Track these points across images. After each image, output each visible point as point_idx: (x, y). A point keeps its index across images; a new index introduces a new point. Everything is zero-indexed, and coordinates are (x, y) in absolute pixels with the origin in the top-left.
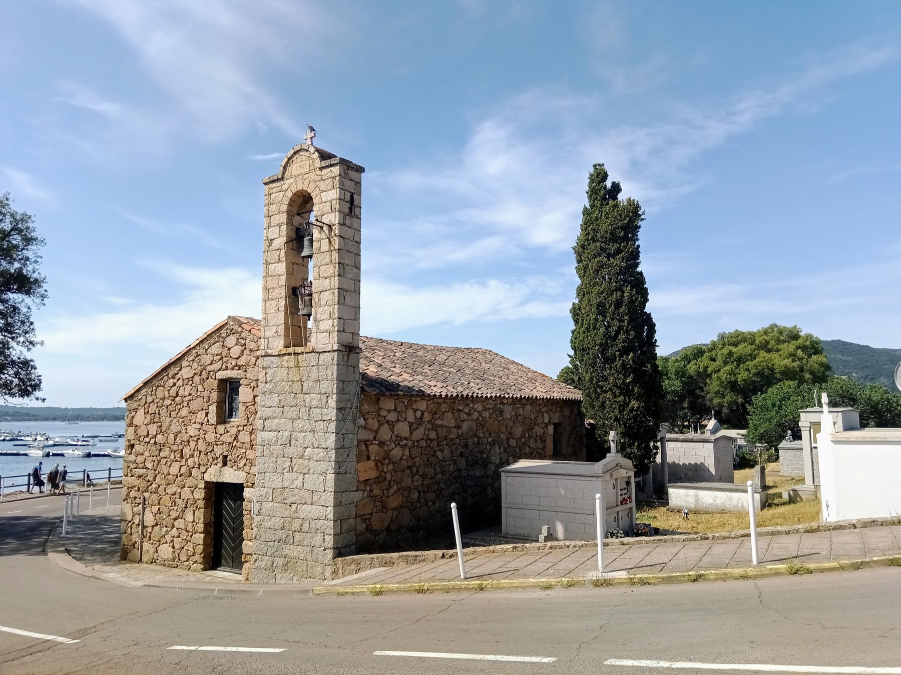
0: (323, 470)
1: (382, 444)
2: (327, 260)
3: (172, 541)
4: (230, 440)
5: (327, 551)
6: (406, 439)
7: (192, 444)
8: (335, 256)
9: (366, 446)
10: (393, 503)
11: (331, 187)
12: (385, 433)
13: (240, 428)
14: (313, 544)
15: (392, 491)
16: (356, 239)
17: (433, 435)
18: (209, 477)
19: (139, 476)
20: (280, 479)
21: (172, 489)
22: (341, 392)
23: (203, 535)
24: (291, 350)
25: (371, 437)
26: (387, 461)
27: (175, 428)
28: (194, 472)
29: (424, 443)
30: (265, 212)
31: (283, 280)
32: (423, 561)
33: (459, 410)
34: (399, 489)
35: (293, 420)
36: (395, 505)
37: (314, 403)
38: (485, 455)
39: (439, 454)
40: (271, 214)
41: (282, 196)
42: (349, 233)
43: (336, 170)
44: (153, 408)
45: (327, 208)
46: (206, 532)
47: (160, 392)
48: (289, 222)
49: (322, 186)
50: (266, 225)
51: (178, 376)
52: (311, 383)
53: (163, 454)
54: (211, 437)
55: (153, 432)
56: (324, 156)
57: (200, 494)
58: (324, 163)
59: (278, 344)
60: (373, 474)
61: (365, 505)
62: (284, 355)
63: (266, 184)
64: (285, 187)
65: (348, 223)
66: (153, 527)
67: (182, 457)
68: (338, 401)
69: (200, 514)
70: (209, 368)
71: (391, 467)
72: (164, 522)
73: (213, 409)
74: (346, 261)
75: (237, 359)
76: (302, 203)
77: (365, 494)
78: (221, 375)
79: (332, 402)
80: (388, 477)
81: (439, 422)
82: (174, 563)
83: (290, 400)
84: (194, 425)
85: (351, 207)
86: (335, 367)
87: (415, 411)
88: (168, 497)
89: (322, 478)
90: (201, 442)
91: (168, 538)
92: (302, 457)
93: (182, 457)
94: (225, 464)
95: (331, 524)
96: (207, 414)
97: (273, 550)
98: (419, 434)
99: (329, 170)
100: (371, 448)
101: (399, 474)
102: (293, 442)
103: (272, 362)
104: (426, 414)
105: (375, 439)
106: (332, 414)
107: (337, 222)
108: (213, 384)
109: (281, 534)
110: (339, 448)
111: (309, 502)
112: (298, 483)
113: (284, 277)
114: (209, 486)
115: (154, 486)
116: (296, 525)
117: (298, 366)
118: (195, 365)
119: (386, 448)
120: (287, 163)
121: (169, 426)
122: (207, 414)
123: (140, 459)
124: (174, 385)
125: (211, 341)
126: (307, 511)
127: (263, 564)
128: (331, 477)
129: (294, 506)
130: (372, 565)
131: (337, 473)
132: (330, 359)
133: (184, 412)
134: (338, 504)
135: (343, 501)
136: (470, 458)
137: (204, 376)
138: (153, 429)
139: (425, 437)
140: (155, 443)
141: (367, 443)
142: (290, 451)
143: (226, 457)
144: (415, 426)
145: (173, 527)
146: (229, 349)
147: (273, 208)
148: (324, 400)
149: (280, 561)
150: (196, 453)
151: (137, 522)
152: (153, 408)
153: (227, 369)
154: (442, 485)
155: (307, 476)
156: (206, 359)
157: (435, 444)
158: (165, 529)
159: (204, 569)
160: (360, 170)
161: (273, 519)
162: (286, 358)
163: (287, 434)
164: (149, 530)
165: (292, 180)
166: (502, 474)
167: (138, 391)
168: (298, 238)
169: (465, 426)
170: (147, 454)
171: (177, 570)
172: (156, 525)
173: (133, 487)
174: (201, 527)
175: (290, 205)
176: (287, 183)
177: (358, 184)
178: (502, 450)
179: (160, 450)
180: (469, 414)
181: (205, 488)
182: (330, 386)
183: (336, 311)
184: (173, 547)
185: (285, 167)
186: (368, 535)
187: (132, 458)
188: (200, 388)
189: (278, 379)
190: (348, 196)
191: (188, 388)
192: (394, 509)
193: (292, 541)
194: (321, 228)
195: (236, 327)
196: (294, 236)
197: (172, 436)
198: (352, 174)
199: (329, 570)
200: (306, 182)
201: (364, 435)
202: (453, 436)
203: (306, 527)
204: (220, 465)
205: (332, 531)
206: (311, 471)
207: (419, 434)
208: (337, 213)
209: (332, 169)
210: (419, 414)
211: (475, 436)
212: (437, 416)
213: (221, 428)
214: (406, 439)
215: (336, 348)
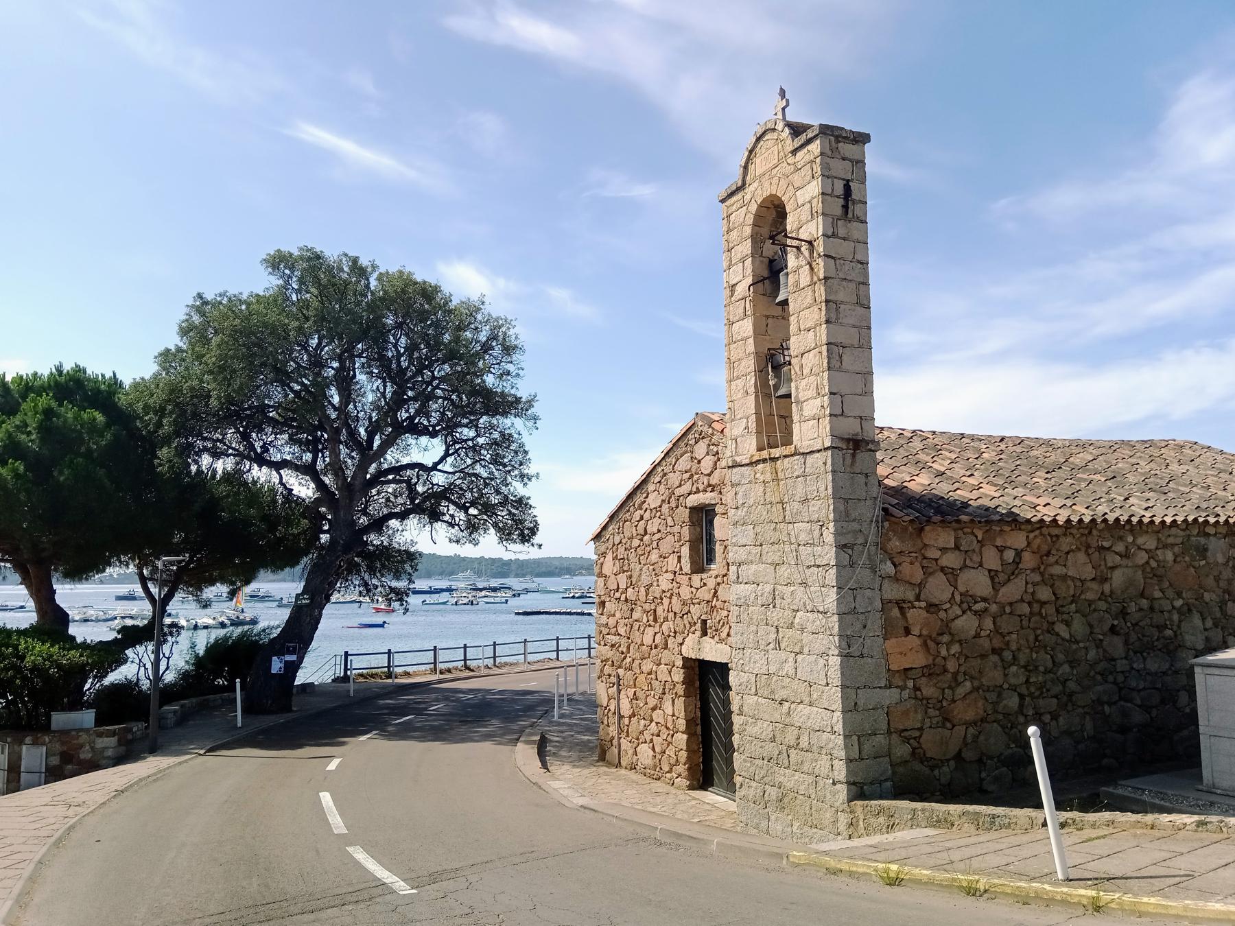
0: (823, 649)
1: (932, 607)
2: (809, 300)
3: (652, 740)
4: (708, 597)
5: (839, 786)
6: (984, 600)
7: (666, 601)
8: (821, 289)
9: (901, 609)
10: (966, 711)
11: (808, 178)
12: (938, 588)
13: (719, 580)
14: (817, 772)
15: (961, 691)
16: (859, 257)
17: (1044, 594)
18: (689, 651)
19: (613, 646)
20: (764, 661)
21: (648, 666)
22: (843, 516)
23: (685, 736)
24: (765, 454)
25: (910, 595)
26: (945, 638)
27: (646, 579)
28: (670, 641)
29: (1025, 609)
30: (724, 246)
31: (751, 347)
32: (1008, 826)
33: (1101, 549)
34: (975, 689)
35: (776, 565)
36: (970, 715)
37: (803, 537)
38: (1169, 633)
39: (1061, 629)
40: (731, 245)
41: (744, 214)
42: (844, 249)
43: (815, 147)
44: (621, 553)
45: (805, 213)
46: (689, 731)
47: (629, 529)
48: (757, 252)
49: (797, 179)
50: (725, 265)
51: (645, 506)
52: (796, 506)
53: (636, 616)
54: (685, 592)
55: (623, 586)
56: (797, 130)
57: (678, 676)
58: (798, 142)
59: (749, 447)
60: (918, 660)
61: (906, 713)
62: (758, 462)
63: (723, 201)
64: (748, 197)
65: (842, 232)
66: (630, 717)
67: (655, 620)
68: (837, 534)
69: (680, 703)
70: (678, 492)
71: (955, 648)
72: (641, 712)
73: (685, 551)
74: (841, 296)
75: (709, 475)
76: (773, 216)
77: (906, 694)
78: (693, 500)
79: (829, 537)
80: (951, 666)
81: (1058, 570)
82: (655, 773)
83: (768, 533)
84: (666, 575)
85: (846, 203)
86: (830, 476)
87: (1001, 550)
88: (643, 676)
89: (822, 662)
90: (675, 598)
91: (647, 736)
92: (791, 626)
93: (655, 620)
94: (704, 633)
95: (840, 740)
96: (679, 557)
97: (763, 772)
98: (1012, 591)
99: (805, 150)
100: (911, 614)
101: (976, 663)
102: (778, 602)
103: (742, 475)
104: (1026, 556)
105: (918, 599)
106: (829, 554)
107: (820, 233)
108: (683, 514)
109: (771, 749)
110: (846, 614)
111: (806, 701)
112: (789, 668)
113: (751, 341)
114: (689, 664)
115: (628, 660)
116: (790, 739)
117: (776, 479)
118: (662, 489)
119: (942, 614)
120: (748, 159)
121: (640, 576)
122: (679, 557)
123: (612, 622)
124: (642, 518)
125: (678, 452)
126: (803, 714)
127: (751, 792)
128: (835, 661)
129: (786, 705)
130: (913, 823)
131: (846, 656)
132: (821, 463)
133: (654, 557)
134: (850, 709)
135: (861, 703)
136: (1133, 637)
137: (673, 504)
138: (623, 580)
139: (1028, 598)
140: (626, 600)
141: (900, 604)
142: (775, 616)
143: (704, 622)
144: (1002, 577)
145: (652, 721)
146: (699, 462)
147: (734, 234)
148: (816, 533)
149: (773, 793)
150: (671, 615)
151: (613, 709)
152: (621, 553)
153: (698, 491)
154: (1072, 685)
155: (800, 657)
156: (674, 479)
157: (1051, 610)
158: (643, 722)
159: (691, 788)
160: (861, 139)
161: (759, 723)
162: (760, 466)
163: (768, 588)
164: (626, 721)
165: (755, 185)
166: (1197, 670)
167: (605, 528)
168: (770, 275)
169: (1118, 577)
170: (618, 615)
171: (658, 783)
172: (633, 715)
173: (607, 660)
174: (682, 724)
175: (755, 225)
176: (749, 190)
177: (860, 163)
178: (1209, 623)
179: (632, 610)
180: (1125, 556)
181: (684, 667)
182: (823, 508)
183: (826, 382)
184: (653, 749)
185: (746, 167)
186: (917, 766)
187: (604, 619)
188: (670, 522)
189: (751, 502)
190: (839, 188)
191: (657, 521)
192: (968, 724)
193: (786, 761)
194: (798, 248)
195: (706, 428)
196: (766, 274)
197: (643, 590)
198: (847, 149)
199: (843, 819)
200: (775, 180)
201: (893, 591)
202: (1090, 596)
203: (804, 743)
204: (698, 633)
205: (843, 754)
206: (806, 650)
207: (1012, 591)
208: (820, 218)
209: (810, 147)
210: (1010, 556)
211: (1142, 595)
212: (1052, 559)
213: (696, 579)
214: (984, 600)
215: (828, 444)
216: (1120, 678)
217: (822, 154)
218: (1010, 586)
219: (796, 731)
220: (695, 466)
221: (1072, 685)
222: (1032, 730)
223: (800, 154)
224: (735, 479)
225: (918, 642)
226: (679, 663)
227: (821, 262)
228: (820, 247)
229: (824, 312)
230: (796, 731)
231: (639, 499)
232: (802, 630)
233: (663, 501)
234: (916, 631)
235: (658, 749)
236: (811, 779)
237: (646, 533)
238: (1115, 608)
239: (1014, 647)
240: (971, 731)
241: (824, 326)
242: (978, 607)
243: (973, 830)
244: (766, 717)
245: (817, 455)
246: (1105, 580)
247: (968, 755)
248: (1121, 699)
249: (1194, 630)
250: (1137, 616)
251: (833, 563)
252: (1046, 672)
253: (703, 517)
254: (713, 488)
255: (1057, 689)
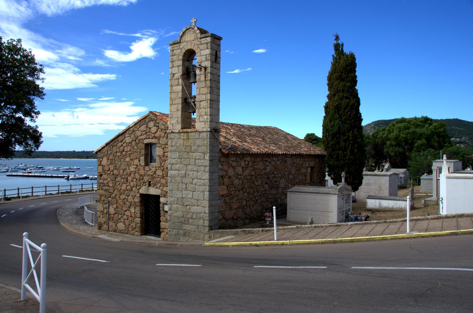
0: (203, 190)
1: (230, 177)
2: (204, 85)
3: (124, 221)
4: (151, 174)
5: (206, 228)
6: (241, 175)
7: (132, 175)
8: (208, 83)
9: (222, 178)
10: (235, 206)
11: (206, 48)
12: (231, 172)
13: (157, 168)
14: (198, 224)
15: (234, 200)
16: (218, 74)
17: (253, 173)
18: (141, 191)
19: (106, 190)
20: (181, 194)
21: (123, 197)
22: (211, 151)
23: (140, 219)
24: (185, 130)
25: (225, 174)
26: (232, 186)
27: (123, 167)
28: (134, 189)
29: (249, 177)
30: (170, 60)
31: (180, 95)
32: (253, 233)
33: (266, 161)
34: (237, 199)
35: (187, 165)
36: (236, 207)
37: (198, 157)
38: (277, 183)
39: (256, 182)
40: (173, 60)
41: (180, 52)
42: (216, 71)
43: (209, 39)
44: (111, 157)
45: (204, 58)
46: (141, 217)
47: (115, 149)
48: (183, 65)
49: (201, 47)
50: (171, 66)
51: (124, 141)
52: (196, 147)
53: (117, 180)
54: (142, 172)
55: (112, 169)
56: (203, 32)
57: (137, 200)
58: (202, 36)
59: (178, 127)
60: (225, 192)
61: (222, 207)
62: (181, 132)
63: (171, 45)
64: (181, 47)
65: (214, 67)
66: (114, 214)
67: (127, 181)
68: (210, 157)
69: (138, 209)
70: (140, 138)
71: (234, 189)
72: (120, 212)
73: (142, 158)
74: (214, 86)
75: (154, 133)
76: (190, 55)
77: (222, 201)
78: (146, 141)
79: (207, 157)
80: (232, 193)
81: (256, 167)
82: (125, 231)
83: (185, 155)
84: (133, 166)
85: (216, 58)
86: (209, 140)
87: (245, 161)
88: (121, 200)
89: (202, 194)
90: (137, 174)
91: (122, 220)
92: (192, 183)
93: (127, 181)
94: (150, 185)
95: (207, 215)
96: (139, 161)
97: (178, 227)
98: (247, 172)
99: (205, 39)
100: (225, 179)
101: (237, 192)
102: (187, 176)
103: (175, 136)
104: (250, 163)
105: (226, 174)
106: (207, 163)
107: (209, 66)
108: (143, 146)
109: (181, 219)
110: (211, 180)
111: (196, 205)
112: (190, 196)
113: (181, 93)
114: (142, 196)
115: (114, 195)
116: (189, 216)
117: (188, 139)
118: (132, 136)
119: (232, 179)
120: (183, 35)
121: (120, 166)
122: (139, 161)
123: (105, 182)
124: (122, 145)
125: (141, 124)
126: (194, 209)
127: (173, 233)
128: (207, 193)
129: (188, 207)
130: (228, 235)
131: (210, 191)
132: (206, 136)
133: (128, 159)
134: (210, 206)
135: (213, 204)
136: (270, 184)
137: (137, 141)
138: (112, 167)
139: (250, 174)
140: (113, 174)
141: (222, 177)
142: (185, 180)
143: (150, 182)
144: (245, 169)
145: (124, 215)
146: (150, 128)
147: (175, 57)
148: (203, 156)
149: (182, 232)
150: (134, 180)
151: (105, 212)
152: (111, 157)
153: (149, 138)
154: (257, 198)
155: (194, 193)
156: (138, 133)
157: (253, 177)
158: (120, 216)
159: (141, 235)
160: (220, 39)
161: (178, 213)
162: (182, 134)
163: (184, 172)
164: (112, 216)
165: (185, 44)
166: (288, 193)
167: (103, 148)
168: (188, 74)
169: (268, 169)
170: (109, 179)
171: (127, 235)
172: (116, 213)
173: (103, 195)
174: (139, 215)
175: (184, 56)
176: (182, 45)
177: (219, 46)
178: (285, 180)
179: (116, 178)
180: (270, 163)
181: (140, 197)
182: (206, 149)
183: (209, 111)
184: (125, 224)
185: (181, 37)
186: (224, 221)
187: (102, 181)
188: (135, 147)
189: (178, 145)
190: (214, 52)
191: (129, 147)
192: (236, 209)
193: (187, 223)
194: (201, 69)
195: (154, 117)
196: (185, 72)
197: (121, 171)
198: (216, 41)
199: (207, 236)
200: (193, 45)
201: (221, 173)
202: (262, 174)
203: (194, 216)
204: (147, 186)
205: (208, 219)
206: (197, 190)
207: (247, 172)
208: (209, 62)
209: (207, 38)
210: (247, 163)
211: (273, 173)
212: (255, 164)
213: (147, 168)
214: (241, 175)
215: (209, 130)
216: (267, 195)
217: (211, 42)
218: (246, 171)
219: (192, 214)
220: (148, 130)
221: (257, 198)
222: (274, 207)
223: (202, 39)
224: (171, 137)
225: (226, 187)
226: (138, 195)
227: (209, 74)
228: (209, 70)
229: (209, 90)
230: (192, 214)
231: (120, 138)
232: (195, 185)
233: (132, 140)
234: (226, 184)
235: (127, 224)
236: (196, 227)
237: (123, 151)
238: (267, 177)
239: (246, 188)
240: (236, 211)
241: (209, 95)
242: (239, 177)
243: (244, 235)
244: (180, 210)
245: (205, 133)
246: (266, 169)
247: (235, 217)
248: (267, 201)
249: (282, 183)
250: (271, 179)
251: (208, 165)
252: (253, 194)
253: (149, 146)
254: (156, 138)
255: (254, 199)
